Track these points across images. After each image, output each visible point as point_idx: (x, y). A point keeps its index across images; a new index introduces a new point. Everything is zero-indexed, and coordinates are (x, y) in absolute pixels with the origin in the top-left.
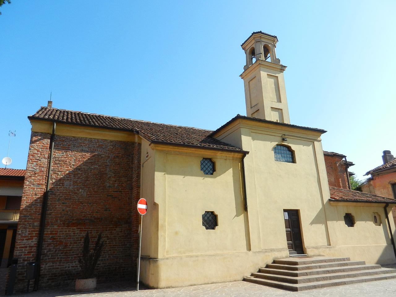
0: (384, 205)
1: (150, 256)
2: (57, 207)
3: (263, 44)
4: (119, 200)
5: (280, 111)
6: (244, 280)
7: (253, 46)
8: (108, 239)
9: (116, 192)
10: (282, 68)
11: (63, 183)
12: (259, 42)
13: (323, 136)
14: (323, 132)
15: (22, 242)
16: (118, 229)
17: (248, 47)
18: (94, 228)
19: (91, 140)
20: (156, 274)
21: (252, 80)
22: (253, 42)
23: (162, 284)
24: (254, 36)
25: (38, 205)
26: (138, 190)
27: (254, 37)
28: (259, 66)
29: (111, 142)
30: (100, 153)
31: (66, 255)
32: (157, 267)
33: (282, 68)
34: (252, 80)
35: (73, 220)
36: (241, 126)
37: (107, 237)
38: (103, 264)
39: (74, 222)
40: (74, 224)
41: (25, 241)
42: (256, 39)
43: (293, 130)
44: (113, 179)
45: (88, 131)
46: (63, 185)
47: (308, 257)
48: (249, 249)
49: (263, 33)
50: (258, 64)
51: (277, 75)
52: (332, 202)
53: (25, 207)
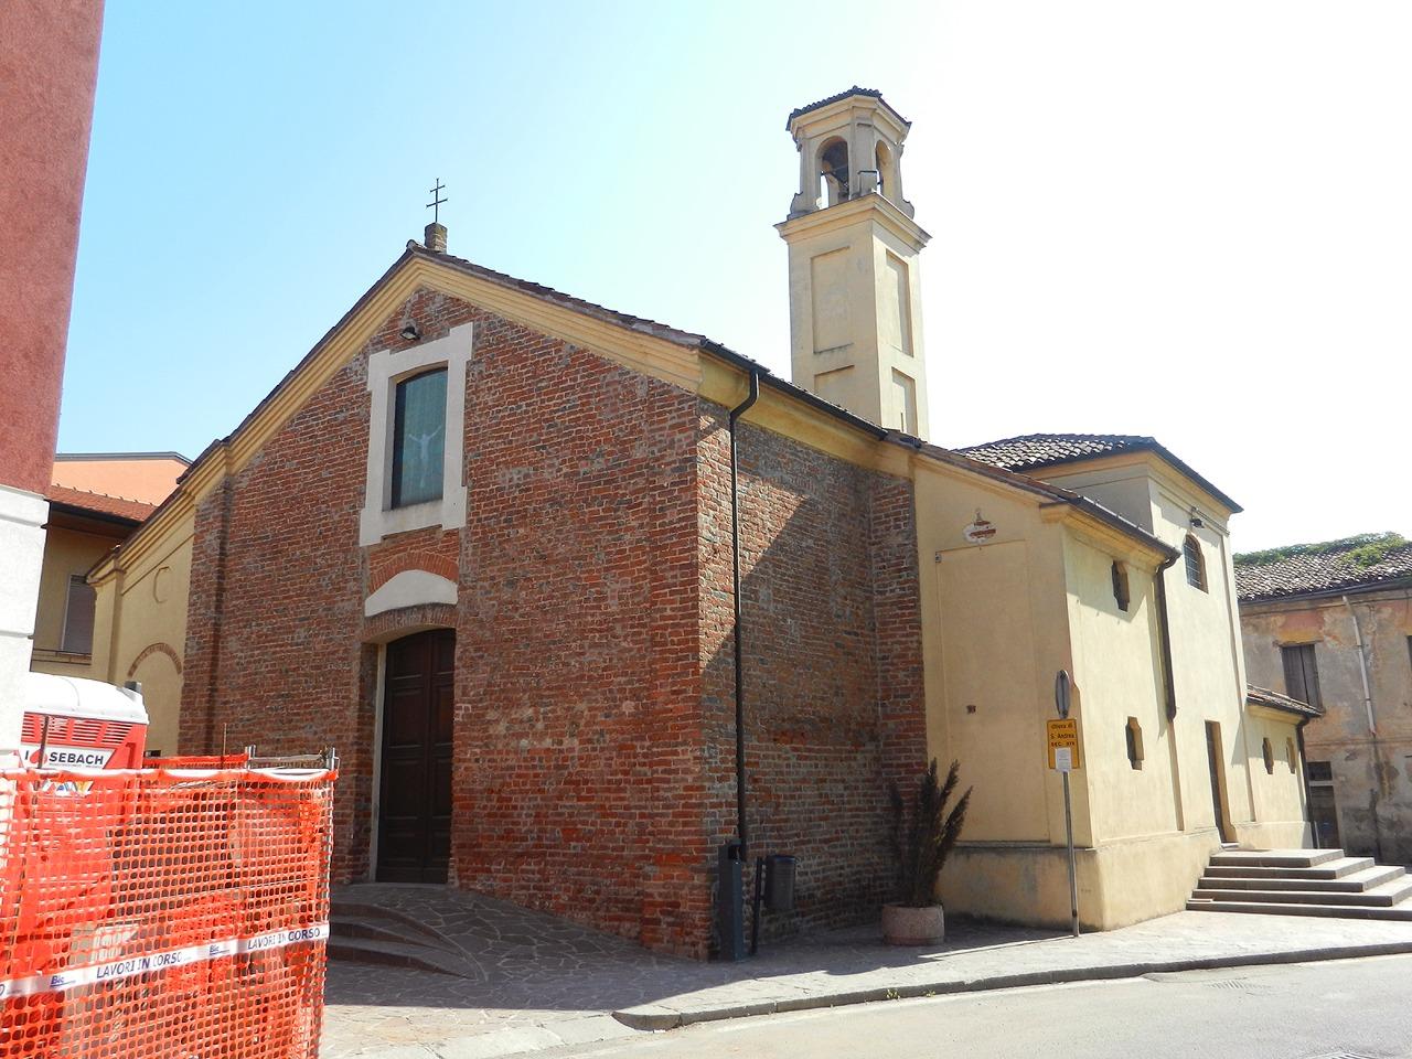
0: (1300, 718)
1: (1049, 841)
2: (752, 672)
3: (878, 137)
4: (856, 662)
5: (908, 383)
6: (1190, 907)
7: (845, 134)
8: (846, 788)
9: (849, 633)
10: (920, 239)
11: (755, 592)
12: (867, 129)
13: (1233, 517)
14: (1236, 509)
15: (713, 788)
16: (859, 756)
17: (823, 129)
18: (819, 751)
19: (794, 446)
20: (1095, 890)
21: (825, 254)
22: (846, 119)
23: (1108, 920)
24: (856, 100)
25: (729, 663)
26: (918, 634)
27: (857, 105)
28: (868, 215)
29: (831, 460)
30: (813, 496)
31: (780, 837)
32: (1095, 871)
33: (920, 239)
34: (825, 254)
35: (784, 720)
36: (1150, 474)
37: (843, 781)
38: (849, 866)
39: (786, 725)
40: (784, 734)
41: (717, 785)
42: (858, 113)
43: (1206, 498)
44: (842, 592)
45: (798, 416)
46: (757, 600)
47: (1236, 848)
48: (1181, 828)
49: (882, 102)
50: (871, 206)
51: (905, 259)
52: (1255, 707)
53: (708, 667)
